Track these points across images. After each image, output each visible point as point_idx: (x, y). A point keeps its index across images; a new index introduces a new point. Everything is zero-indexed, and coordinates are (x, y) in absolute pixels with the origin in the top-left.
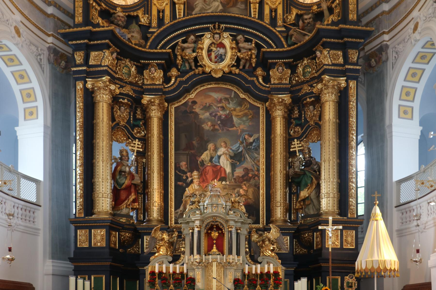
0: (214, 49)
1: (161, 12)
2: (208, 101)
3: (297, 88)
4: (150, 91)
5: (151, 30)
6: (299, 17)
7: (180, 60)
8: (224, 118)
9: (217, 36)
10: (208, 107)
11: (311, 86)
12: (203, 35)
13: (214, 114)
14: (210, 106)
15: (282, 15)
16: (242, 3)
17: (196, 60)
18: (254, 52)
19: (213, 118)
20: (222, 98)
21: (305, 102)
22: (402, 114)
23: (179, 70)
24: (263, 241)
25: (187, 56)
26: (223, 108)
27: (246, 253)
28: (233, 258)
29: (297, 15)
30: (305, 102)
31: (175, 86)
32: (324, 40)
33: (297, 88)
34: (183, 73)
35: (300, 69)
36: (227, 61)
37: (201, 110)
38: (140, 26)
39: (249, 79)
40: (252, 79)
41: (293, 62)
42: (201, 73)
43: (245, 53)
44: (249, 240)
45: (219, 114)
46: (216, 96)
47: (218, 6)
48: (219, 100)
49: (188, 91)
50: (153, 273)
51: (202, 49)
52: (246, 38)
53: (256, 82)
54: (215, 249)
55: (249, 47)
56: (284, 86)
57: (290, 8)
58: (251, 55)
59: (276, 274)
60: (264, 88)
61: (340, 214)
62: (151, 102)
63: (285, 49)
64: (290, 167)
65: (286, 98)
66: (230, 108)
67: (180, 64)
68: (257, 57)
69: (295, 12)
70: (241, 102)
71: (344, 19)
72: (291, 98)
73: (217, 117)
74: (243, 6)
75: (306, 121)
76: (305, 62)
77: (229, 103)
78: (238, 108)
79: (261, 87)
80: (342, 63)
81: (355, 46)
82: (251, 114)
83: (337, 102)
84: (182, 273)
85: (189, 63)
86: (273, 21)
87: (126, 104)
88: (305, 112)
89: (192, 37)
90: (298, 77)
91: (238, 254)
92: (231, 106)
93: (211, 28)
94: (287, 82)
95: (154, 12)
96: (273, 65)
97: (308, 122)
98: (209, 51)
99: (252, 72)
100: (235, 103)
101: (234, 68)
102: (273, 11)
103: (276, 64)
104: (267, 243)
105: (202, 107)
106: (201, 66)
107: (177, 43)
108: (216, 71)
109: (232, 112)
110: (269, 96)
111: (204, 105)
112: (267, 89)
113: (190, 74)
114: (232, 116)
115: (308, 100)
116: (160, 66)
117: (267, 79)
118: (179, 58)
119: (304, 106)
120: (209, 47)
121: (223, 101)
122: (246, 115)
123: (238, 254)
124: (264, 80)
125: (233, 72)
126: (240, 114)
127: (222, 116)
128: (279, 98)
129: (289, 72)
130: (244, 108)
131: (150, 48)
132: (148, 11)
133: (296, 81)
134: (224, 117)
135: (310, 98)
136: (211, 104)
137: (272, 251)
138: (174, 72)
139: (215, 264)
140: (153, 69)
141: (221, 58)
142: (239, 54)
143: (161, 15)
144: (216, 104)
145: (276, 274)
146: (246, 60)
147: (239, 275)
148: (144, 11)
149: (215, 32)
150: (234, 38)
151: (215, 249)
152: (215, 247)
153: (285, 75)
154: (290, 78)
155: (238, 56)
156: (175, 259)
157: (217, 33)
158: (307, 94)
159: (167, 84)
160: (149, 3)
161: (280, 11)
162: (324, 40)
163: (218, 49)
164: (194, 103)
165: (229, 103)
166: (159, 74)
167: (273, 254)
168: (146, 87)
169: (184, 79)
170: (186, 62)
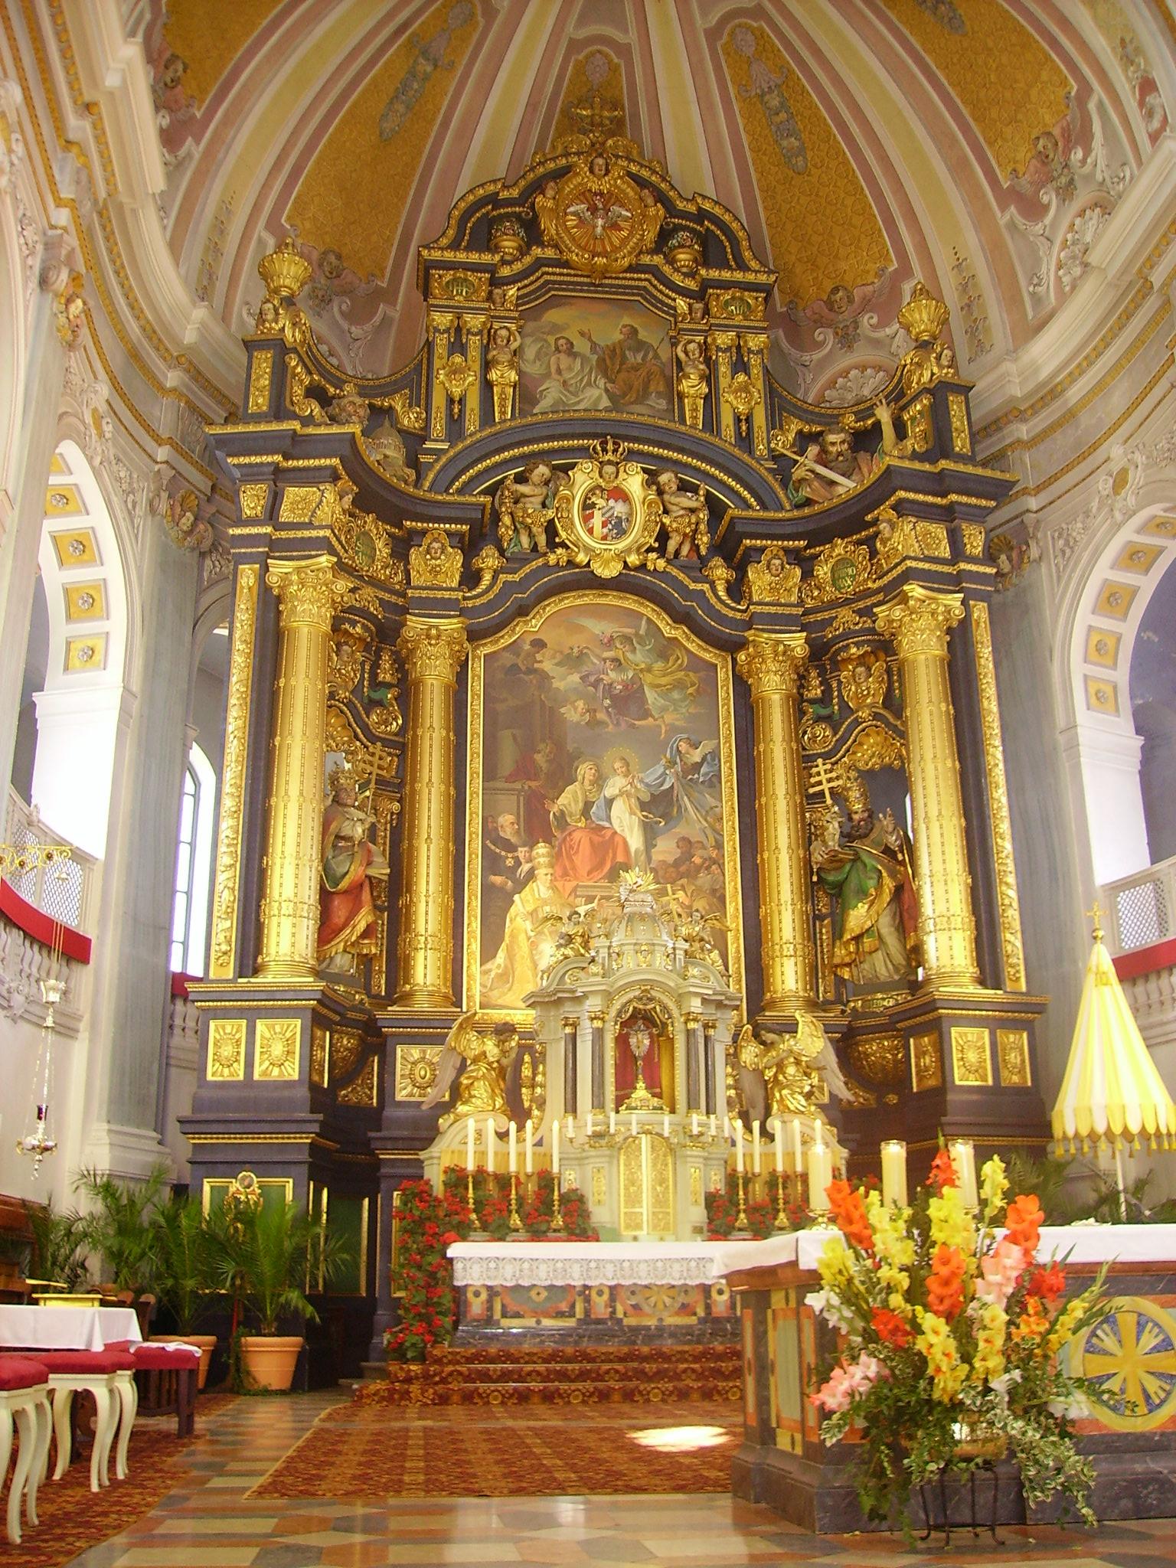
0: (600, 502)
2: (576, 642)
3: (820, 617)
5: (428, 445)
6: (804, 440)
7: (507, 527)
11: (867, 612)
12: (572, 466)
13: (592, 679)
14: (581, 654)
15: (764, 428)
16: (659, 394)
17: (551, 529)
18: (703, 515)
21: (844, 655)
22: (1093, 700)
23: (502, 552)
24: (780, 1067)
25: (529, 516)
26: (617, 663)
27: (730, 1102)
29: (800, 433)
30: (844, 655)
31: (491, 595)
32: (902, 494)
33: (820, 617)
35: (823, 571)
36: (638, 533)
37: (557, 664)
39: (692, 586)
40: (699, 587)
41: (806, 548)
42: (563, 562)
43: (682, 516)
44: (733, 1058)
45: (606, 680)
47: (599, 398)
49: (523, 611)
51: (569, 500)
52: (681, 480)
53: (709, 594)
54: (641, 1092)
55: (693, 504)
56: (787, 611)
57: (780, 415)
58: (697, 524)
60: (731, 614)
61: (982, 982)
63: (788, 515)
65: (797, 642)
67: (507, 538)
69: (794, 426)
70: (666, 649)
71: (940, 445)
72: (807, 640)
74: (663, 404)
76: (839, 550)
78: (659, 665)
79: (725, 611)
80: (947, 555)
81: (978, 516)
82: (693, 685)
83: (942, 660)
85: (531, 535)
87: (361, 639)
88: (840, 683)
89: (542, 470)
90: (818, 588)
92: (639, 657)
93: (594, 448)
94: (794, 599)
95: (438, 400)
97: (852, 711)
98: (587, 506)
99: (698, 567)
101: (653, 556)
103: (762, 550)
104: (791, 1070)
105: (559, 657)
106: (563, 545)
107: (502, 481)
110: (750, 635)
112: (738, 616)
113: (534, 565)
114: (642, 686)
115: (854, 650)
117: (737, 589)
118: (507, 520)
119: (837, 666)
120: (587, 498)
122: (679, 685)
124: (729, 591)
125: (651, 567)
126: (664, 681)
128: (778, 642)
129: (798, 572)
131: (430, 490)
132: (421, 397)
133: (813, 598)
135: (857, 645)
138: (489, 560)
139: (645, 1141)
140: (436, 545)
142: (666, 520)
143: (456, 411)
144: (598, 651)
146: (685, 535)
148: (411, 398)
149: (607, 458)
150: (651, 478)
151: (641, 1092)
152: (641, 1085)
153: (786, 578)
154: (800, 591)
155: (663, 524)
157: (609, 462)
158: (847, 635)
159: (470, 590)
160: (424, 378)
161: (760, 419)
162: (902, 494)
163: (612, 502)
164: (539, 644)
166: (453, 563)
167: (813, 1108)
168: (417, 593)
169: (516, 577)
170: (522, 531)
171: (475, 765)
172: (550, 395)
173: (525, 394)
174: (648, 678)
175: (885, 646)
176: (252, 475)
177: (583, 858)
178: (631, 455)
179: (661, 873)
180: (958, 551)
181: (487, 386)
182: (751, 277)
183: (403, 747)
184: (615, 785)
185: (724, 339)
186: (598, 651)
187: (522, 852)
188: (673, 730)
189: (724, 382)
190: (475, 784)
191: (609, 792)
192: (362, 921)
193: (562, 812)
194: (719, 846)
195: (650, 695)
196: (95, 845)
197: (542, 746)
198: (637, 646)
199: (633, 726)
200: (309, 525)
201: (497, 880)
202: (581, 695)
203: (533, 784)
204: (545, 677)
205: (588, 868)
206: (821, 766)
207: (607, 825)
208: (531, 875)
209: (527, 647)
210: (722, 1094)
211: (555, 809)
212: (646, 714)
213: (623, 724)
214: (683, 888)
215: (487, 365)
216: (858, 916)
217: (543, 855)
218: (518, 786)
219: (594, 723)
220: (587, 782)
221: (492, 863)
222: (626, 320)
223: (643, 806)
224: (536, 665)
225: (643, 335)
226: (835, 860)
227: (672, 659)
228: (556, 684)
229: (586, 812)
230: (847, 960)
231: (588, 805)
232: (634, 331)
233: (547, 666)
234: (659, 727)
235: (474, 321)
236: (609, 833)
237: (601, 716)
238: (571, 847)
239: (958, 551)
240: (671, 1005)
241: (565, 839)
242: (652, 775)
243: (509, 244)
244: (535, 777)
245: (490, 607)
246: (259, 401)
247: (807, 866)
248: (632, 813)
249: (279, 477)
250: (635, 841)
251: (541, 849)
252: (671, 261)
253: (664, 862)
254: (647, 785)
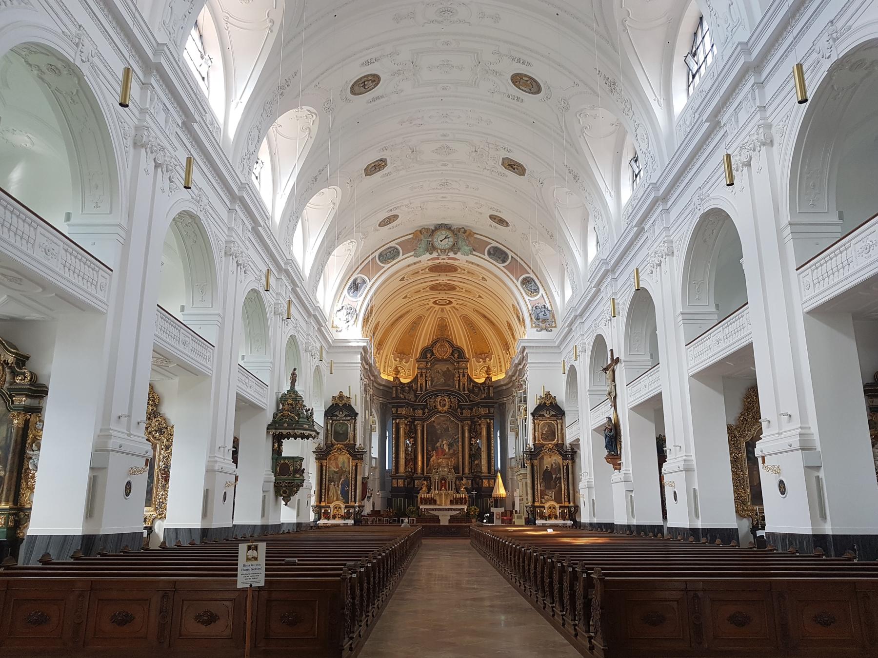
1: (421, 384)
4: (418, 419)
5: (418, 392)
9: (443, 397)
12: (438, 396)
17: (435, 406)
23: (428, 410)
24: (461, 484)
28: (450, 492)
29: (473, 385)
34: (430, 411)
36: (447, 407)
38: (413, 390)
44: (455, 484)
46: (442, 419)
50: (421, 498)
59: (465, 498)
62: (418, 424)
64: (471, 450)
65: (469, 422)
68: (458, 404)
74: (452, 381)
75: (477, 431)
76: (476, 408)
78: (451, 424)
84: (432, 497)
86: (464, 388)
91: (452, 490)
92: (448, 423)
95: (419, 385)
96: (464, 409)
98: (440, 402)
102: (464, 384)
108: (443, 410)
116: (421, 409)
117: (462, 413)
123: (452, 490)
132: (417, 384)
137: (465, 488)
138: (427, 410)
141: (444, 405)
145: (465, 498)
147: (452, 499)
150: (449, 398)
156: (429, 491)
161: (466, 384)
164: (434, 421)
166: (421, 412)
171: (425, 440)
172: (436, 380)
173: (432, 381)
175: (480, 425)
176: (393, 407)
177: (440, 453)
178: (447, 394)
180: (489, 413)
181: (426, 381)
182: (465, 360)
183: (415, 439)
184: (445, 442)
185: (461, 371)
188: (453, 434)
189: (461, 378)
190: (425, 443)
192: (411, 463)
194: (459, 450)
196: (377, 457)
200: (402, 414)
201: (428, 456)
204: (435, 427)
206: (473, 439)
208: (433, 456)
210: (453, 488)
215: (426, 377)
216: (476, 462)
221: (428, 454)
222: (447, 366)
223: (448, 445)
225: (450, 369)
226: (473, 454)
228: (437, 427)
229: (440, 446)
231: (441, 445)
232: (448, 368)
233: (435, 425)
235: (424, 371)
239: (489, 413)
243: (429, 356)
245: (426, 418)
246: (394, 395)
247: (470, 454)
249: (397, 407)
250: (447, 450)
251: (434, 452)
252: (454, 356)
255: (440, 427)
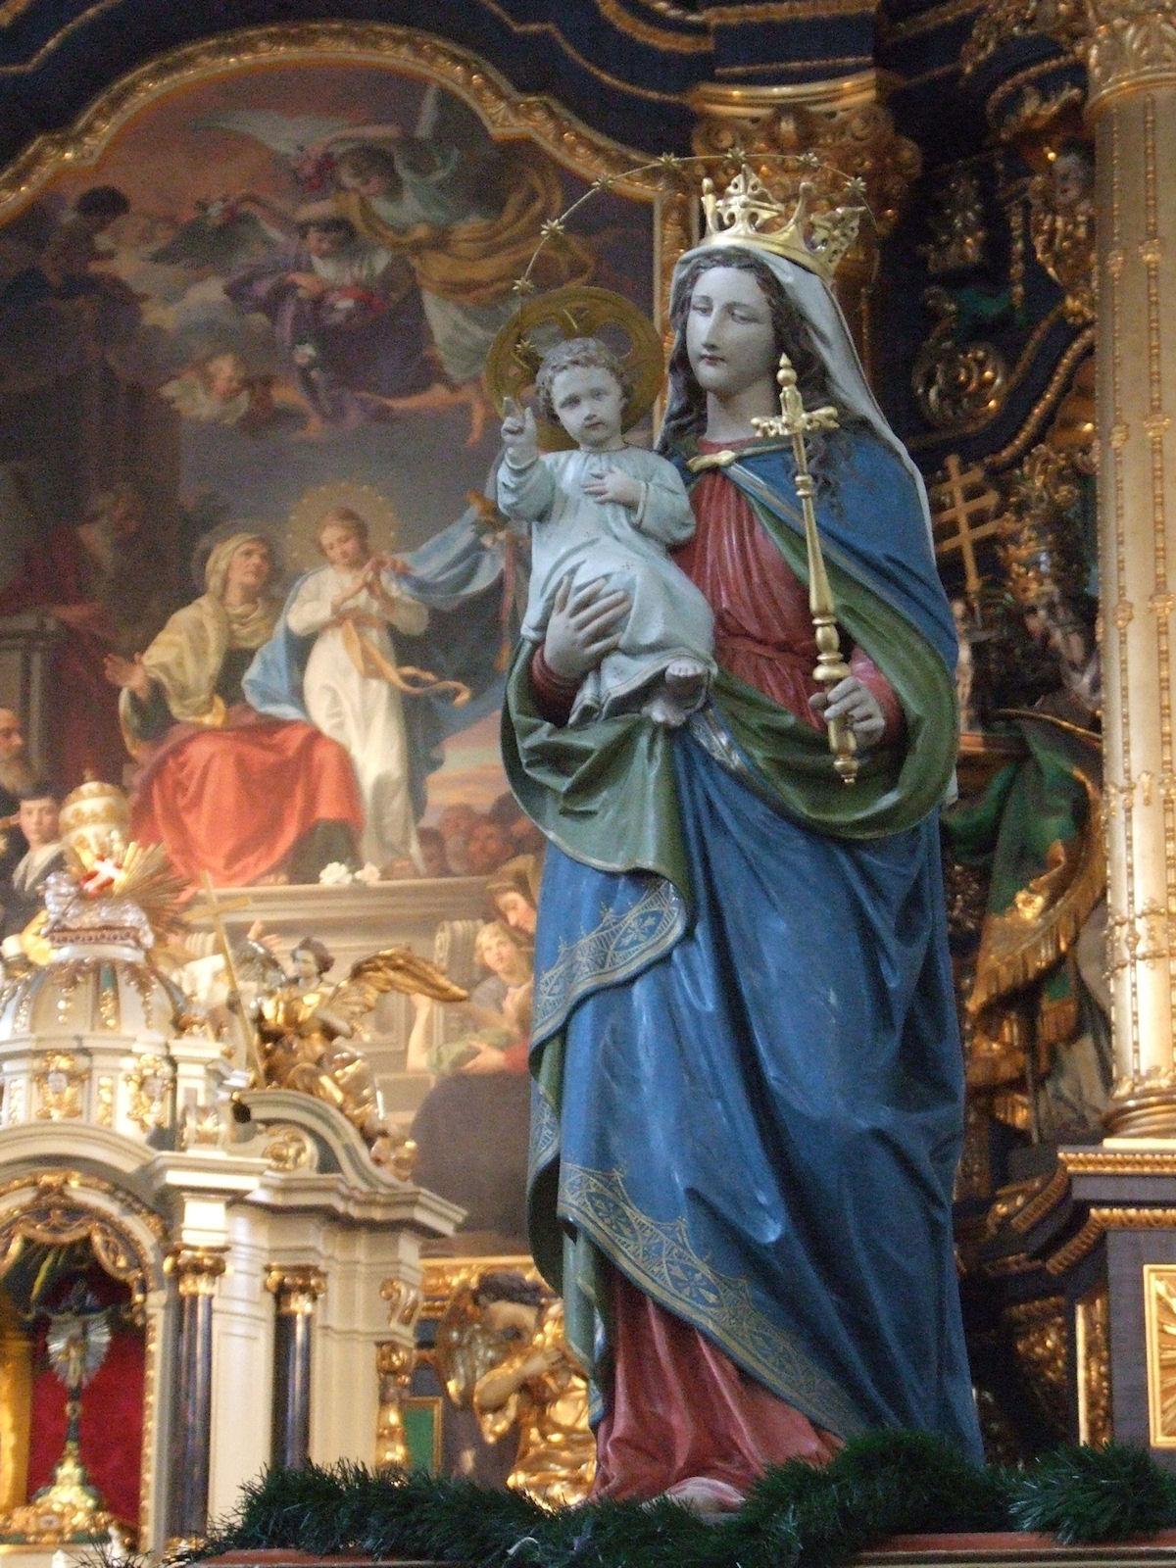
8: (350, 315)
10: (221, 230)
13: (263, 288)
19: (259, 319)
20: (341, 150)
26: (343, 235)
48: (309, 169)
66: (403, 231)
73: (288, 312)
77: (394, 191)
78: (470, 226)
100: (440, 186)
105: (163, 237)
109: (415, 263)
111: (188, 215)
114: (414, 295)
121: (347, 178)
126: (486, 270)
127: (331, 298)
130: (518, 218)
134: (345, 304)
136: (245, 208)
144: (282, 204)
165: (394, 191)
174: (436, 267)
179: (453, 843)
186: (282, 204)
187: (31, 815)
191: (300, 615)
193: (157, 689)
195: (441, 318)
197: (101, 501)
198: (406, 175)
199: (383, 415)
202: (221, 337)
203: (73, 614)
204: (120, 299)
205: (228, 845)
207: (288, 712)
209: (68, 217)
211: (133, 682)
212: (428, 374)
213: (354, 417)
214: (522, 884)
217: (95, 818)
218: (28, 622)
219: (265, 419)
220: (234, 595)
223: (405, 648)
224: (95, 268)
227: (514, 200)
228: (159, 315)
229: (228, 683)
230: (1006, 1070)
231: (236, 660)
234: (465, 408)
236: (295, 739)
237: (288, 395)
238: (180, 787)
240: (143, 1231)
241: (159, 770)
242: (433, 562)
244: (80, 596)
248: (371, 671)
251: (91, 799)
253: (465, 811)
254: (421, 587)
255: (235, 292)
